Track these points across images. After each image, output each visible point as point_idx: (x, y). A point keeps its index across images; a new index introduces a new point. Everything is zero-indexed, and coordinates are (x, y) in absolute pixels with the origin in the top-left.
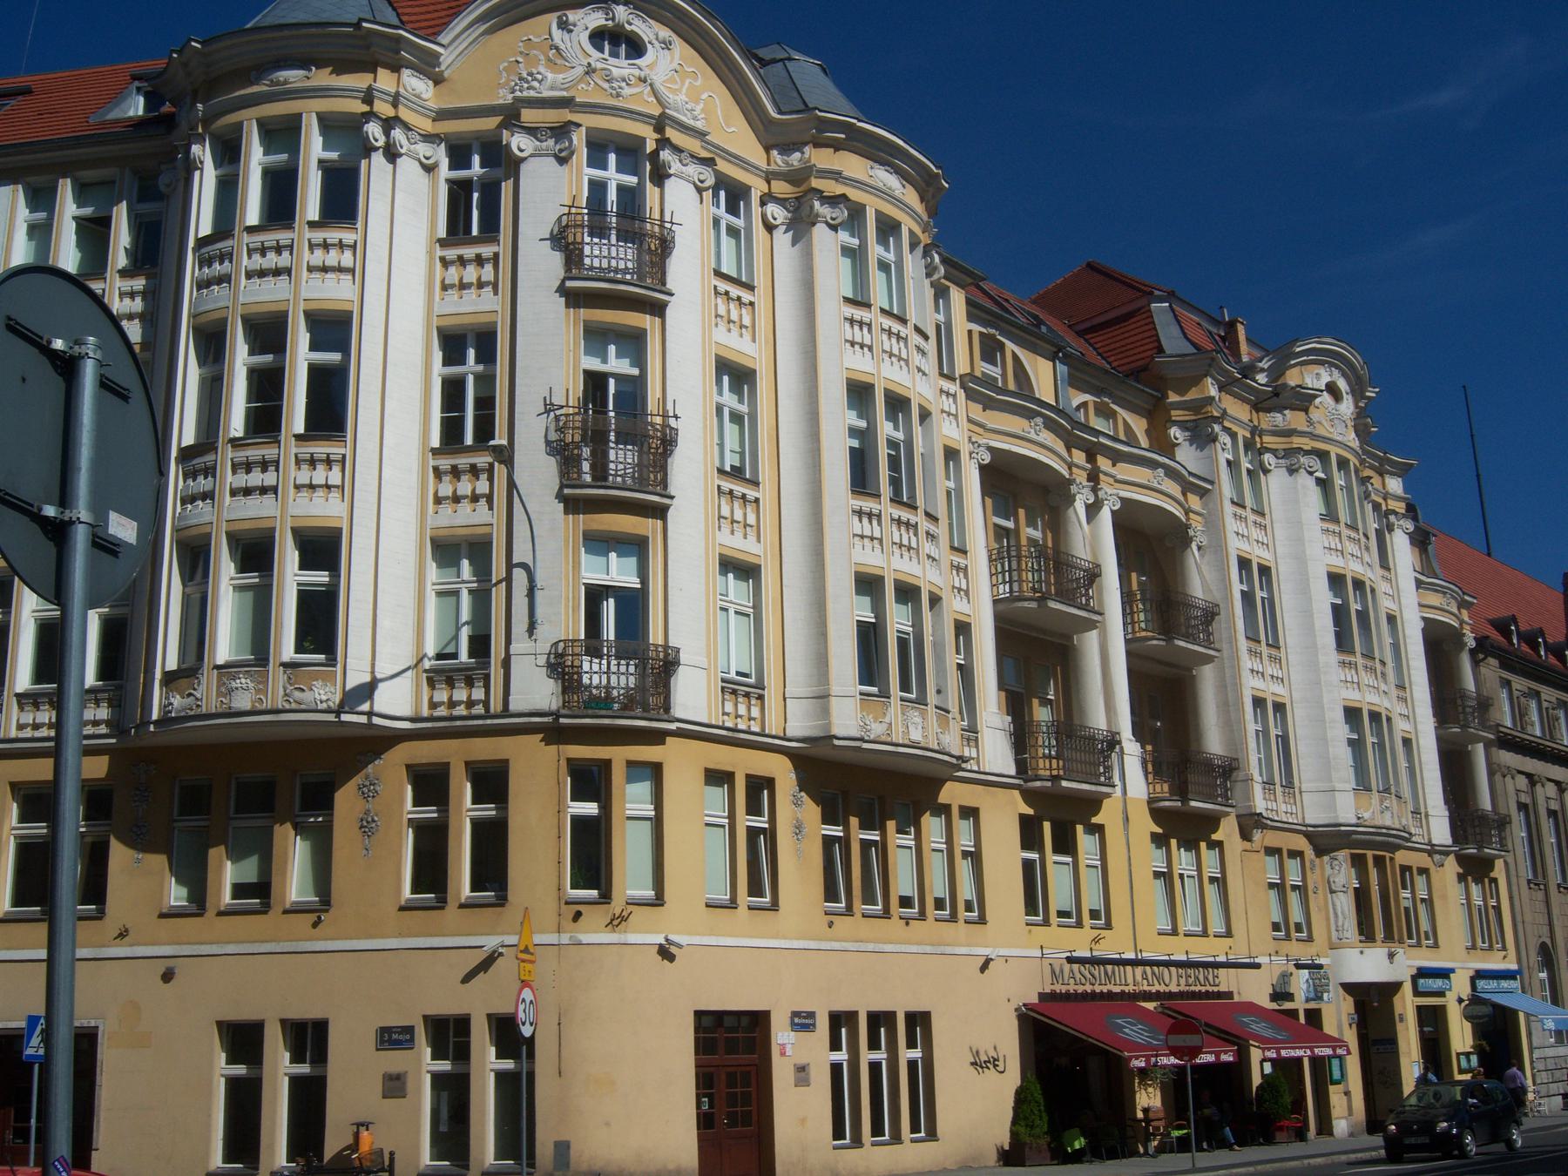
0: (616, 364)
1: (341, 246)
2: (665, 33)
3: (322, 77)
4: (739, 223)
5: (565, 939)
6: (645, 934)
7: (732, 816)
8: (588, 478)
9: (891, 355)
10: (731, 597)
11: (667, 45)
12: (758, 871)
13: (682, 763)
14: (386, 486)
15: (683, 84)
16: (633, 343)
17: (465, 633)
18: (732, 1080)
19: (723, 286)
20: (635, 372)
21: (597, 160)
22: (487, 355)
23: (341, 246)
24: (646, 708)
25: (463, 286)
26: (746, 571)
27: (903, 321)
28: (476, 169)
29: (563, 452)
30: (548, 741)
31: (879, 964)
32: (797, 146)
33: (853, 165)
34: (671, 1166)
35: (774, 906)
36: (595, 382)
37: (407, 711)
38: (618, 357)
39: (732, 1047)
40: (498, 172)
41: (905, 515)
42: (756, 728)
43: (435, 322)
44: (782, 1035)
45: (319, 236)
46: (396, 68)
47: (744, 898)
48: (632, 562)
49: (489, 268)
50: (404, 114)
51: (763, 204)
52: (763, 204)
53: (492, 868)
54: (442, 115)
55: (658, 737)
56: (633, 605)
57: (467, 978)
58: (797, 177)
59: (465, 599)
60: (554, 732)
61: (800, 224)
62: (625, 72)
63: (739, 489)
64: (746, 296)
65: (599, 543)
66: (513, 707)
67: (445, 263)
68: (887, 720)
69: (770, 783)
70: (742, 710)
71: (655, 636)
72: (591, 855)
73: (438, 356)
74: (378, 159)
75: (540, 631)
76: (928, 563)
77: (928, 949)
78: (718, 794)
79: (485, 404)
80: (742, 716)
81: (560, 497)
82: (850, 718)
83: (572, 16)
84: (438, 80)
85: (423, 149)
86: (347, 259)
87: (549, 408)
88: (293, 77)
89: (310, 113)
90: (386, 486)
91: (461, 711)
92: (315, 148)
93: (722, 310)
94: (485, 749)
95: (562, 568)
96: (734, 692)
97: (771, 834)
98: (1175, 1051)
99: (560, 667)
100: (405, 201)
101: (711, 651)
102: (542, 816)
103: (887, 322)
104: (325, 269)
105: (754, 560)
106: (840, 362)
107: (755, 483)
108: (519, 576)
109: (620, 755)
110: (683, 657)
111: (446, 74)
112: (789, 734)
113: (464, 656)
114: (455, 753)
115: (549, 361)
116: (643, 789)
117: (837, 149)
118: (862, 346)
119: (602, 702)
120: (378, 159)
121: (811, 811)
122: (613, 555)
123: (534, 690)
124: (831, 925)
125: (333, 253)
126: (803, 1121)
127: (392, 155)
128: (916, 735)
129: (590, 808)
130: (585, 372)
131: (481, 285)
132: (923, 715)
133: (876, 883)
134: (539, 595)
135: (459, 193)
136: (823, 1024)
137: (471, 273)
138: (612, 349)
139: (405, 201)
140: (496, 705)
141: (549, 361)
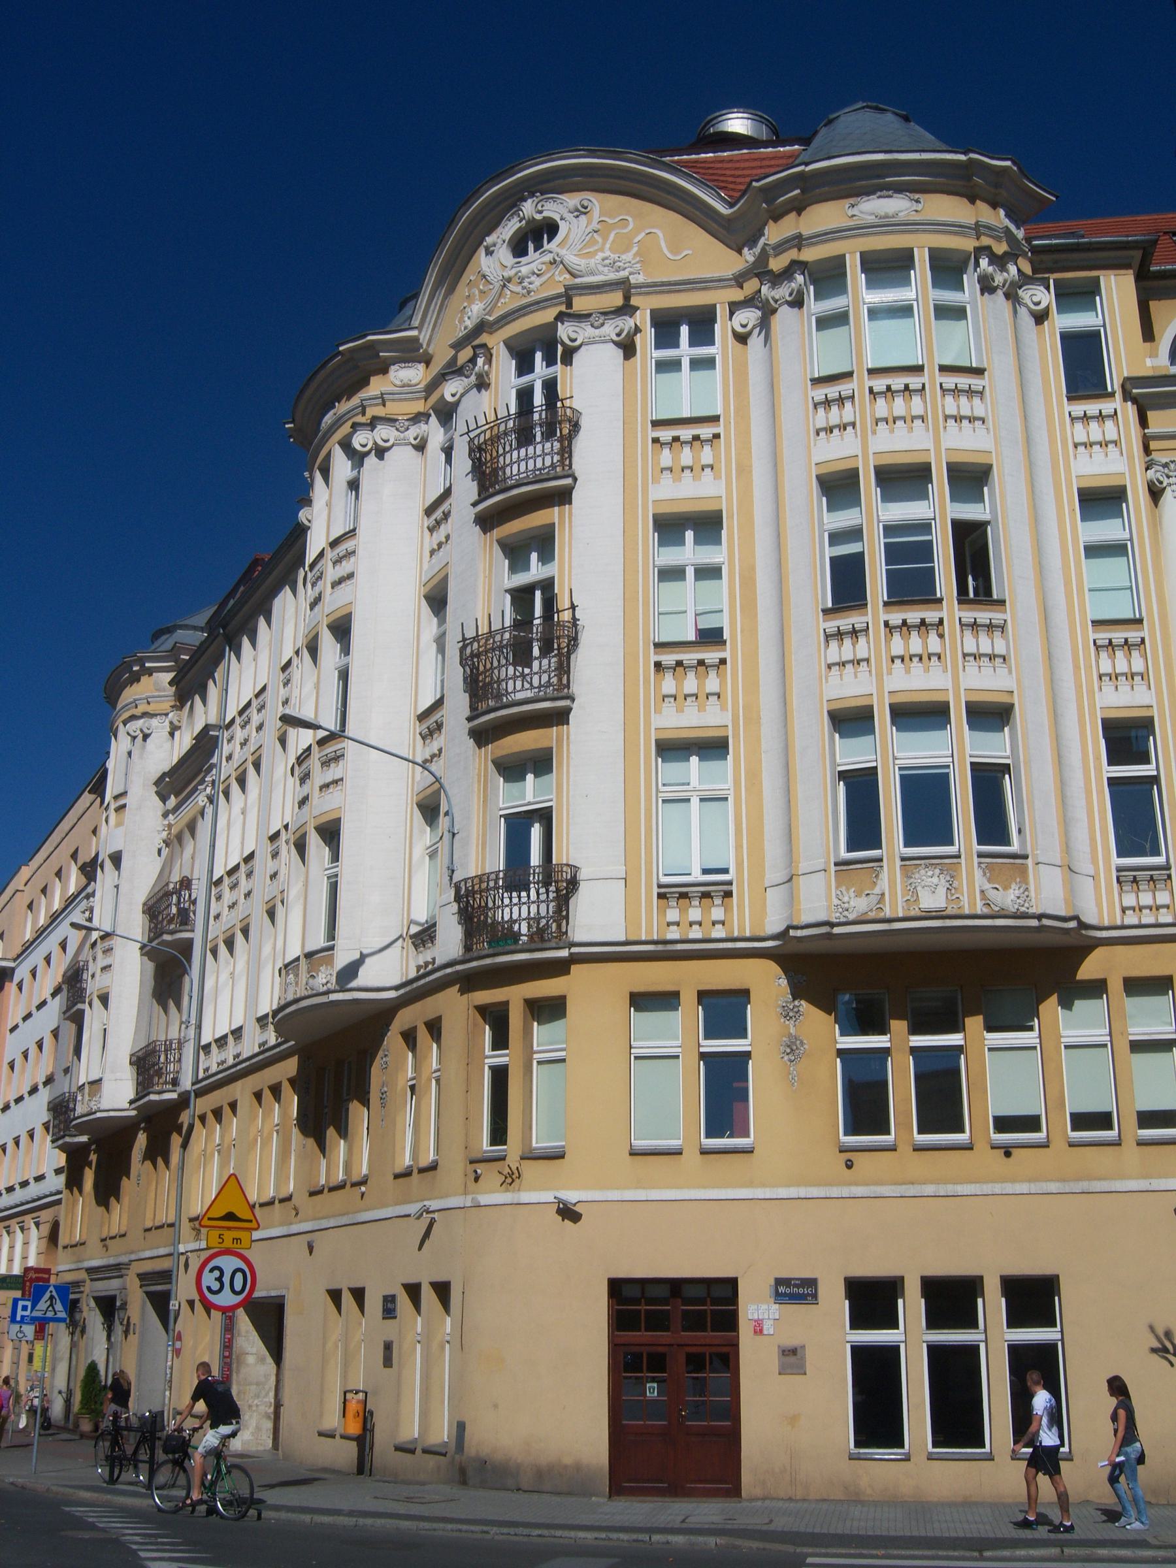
2: (572, 200)
6: (539, 1191)
10: (694, 782)
11: (581, 211)
15: (605, 239)
16: (544, 543)
21: (525, 366)
30: (463, 991)
33: (825, 216)
34: (568, 1460)
36: (521, 597)
37: (397, 981)
39: (695, 1322)
44: (756, 1307)
55: (560, 968)
57: (420, 1249)
60: (469, 982)
62: (533, 266)
65: (512, 769)
68: (877, 890)
77: (1053, 1187)
80: (693, 922)
82: (821, 901)
83: (489, 240)
105: (1004, 699)
109: (515, 995)
111: (431, 351)
117: (799, 211)
122: (694, 760)
124: (849, 1165)
126: (793, 1420)
133: (941, 1100)
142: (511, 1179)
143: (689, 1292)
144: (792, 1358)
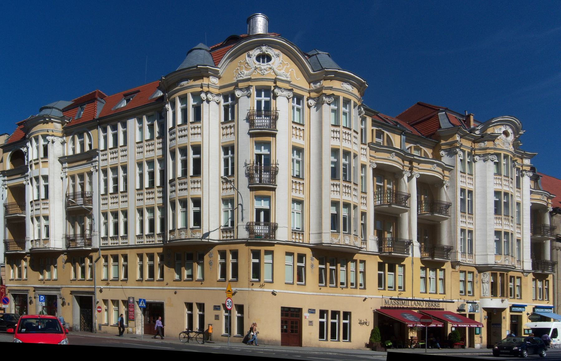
0: (264, 151)
1: (198, 128)
3: (191, 83)
4: (300, 107)
5: (250, 289)
6: (268, 289)
7: (293, 263)
8: (258, 182)
9: (346, 140)
10: (295, 209)
12: (300, 275)
13: (279, 251)
14: (210, 187)
17: (230, 220)
18: (292, 323)
19: (295, 126)
20: (269, 153)
22: (233, 153)
23: (198, 128)
24: (270, 238)
25: (227, 134)
26: (299, 202)
27: (350, 129)
28: (230, 101)
29: (250, 176)
30: (246, 245)
31: (336, 299)
32: (319, 81)
35: (305, 285)
36: (259, 156)
38: (264, 149)
40: (234, 102)
41: (347, 184)
42: (301, 242)
43: (221, 145)
44: (305, 314)
45: (193, 126)
46: (208, 77)
47: (296, 282)
48: (268, 202)
49: (233, 129)
50: (211, 89)
51: (308, 100)
52: (308, 100)
53: (235, 274)
54: (221, 88)
55: (273, 245)
56: (267, 213)
58: (318, 91)
59: (230, 212)
60: (248, 244)
61: (319, 104)
63: (298, 181)
64: (302, 128)
65: (259, 198)
66: (239, 238)
67: (223, 129)
69: (305, 255)
70: (297, 237)
71: (272, 220)
72: (257, 271)
73: (222, 153)
74: (205, 103)
75: (244, 220)
76: (354, 197)
78: (290, 258)
79: (233, 164)
80: (298, 239)
81: (249, 187)
84: (219, 78)
85: (216, 98)
86: (199, 131)
87: (246, 165)
88: (184, 83)
89: (189, 92)
90: (210, 187)
91: (229, 238)
92: (191, 102)
93: (294, 133)
94: (233, 247)
95: (250, 205)
96: (295, 233)
97: (305, 267)
98: (422, 323)
99: (249, 228)
100: (213, 113)
101: (289, 222)
102: (246, 262)
103: (345, 130)
104: (195, 134)
106: (329, 143)
107: (303, 179)
108: (240, 206)
109: (263, 249)
110: (279, 226)
112: (310, 243)
113: (230, 226)
114: (227, 248)
115: (247, 152)
116: (270, 256)
118: (336, 138)
119: (259, 236)
120: (205, 103)
121: (316, 262)
123: (243, 234)
125: (196, 129)
126: (311, 333)
127: (208, 101)
128: (347, 242)
129: (257, 261)
130: (256, 154)
131: (231, 134)
132: (350, 237)
134: (244, 211)
135: (226, 108)
136: (318, 313)
137: (229, 131)
138: (263, 147)
139: (213, 113)
140: (235, 238)
141: (247, 152)
142: (262, 286)
143: (292, 310)
144: (311, 323)
